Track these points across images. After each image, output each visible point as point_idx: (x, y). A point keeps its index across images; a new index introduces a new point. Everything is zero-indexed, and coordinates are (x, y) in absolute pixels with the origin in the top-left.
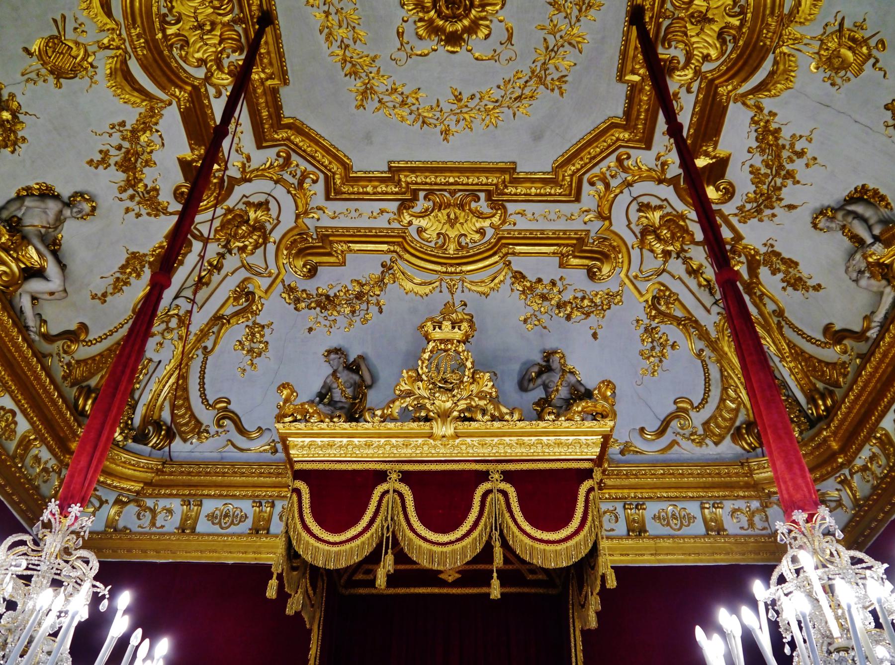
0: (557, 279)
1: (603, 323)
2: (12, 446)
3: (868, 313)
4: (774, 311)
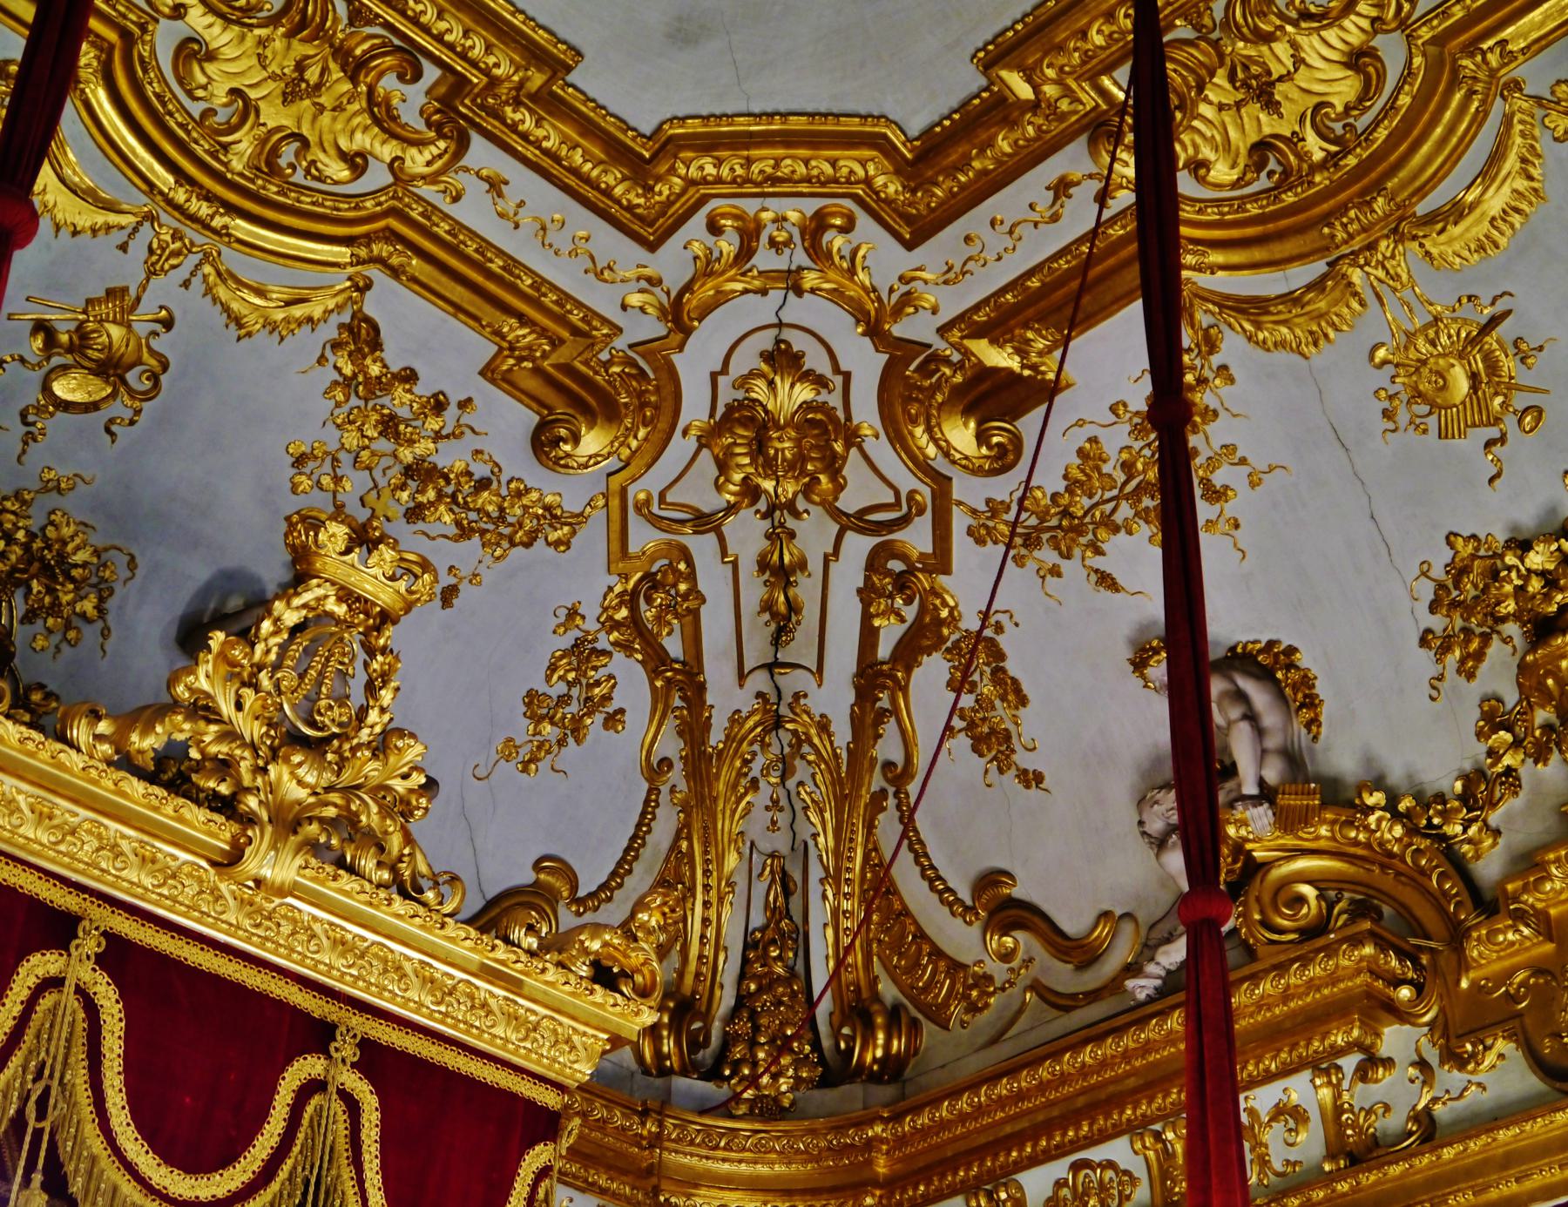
0: (455, 397)
1: (487, 576)
3: (1118, 912)
4: (889, 765)
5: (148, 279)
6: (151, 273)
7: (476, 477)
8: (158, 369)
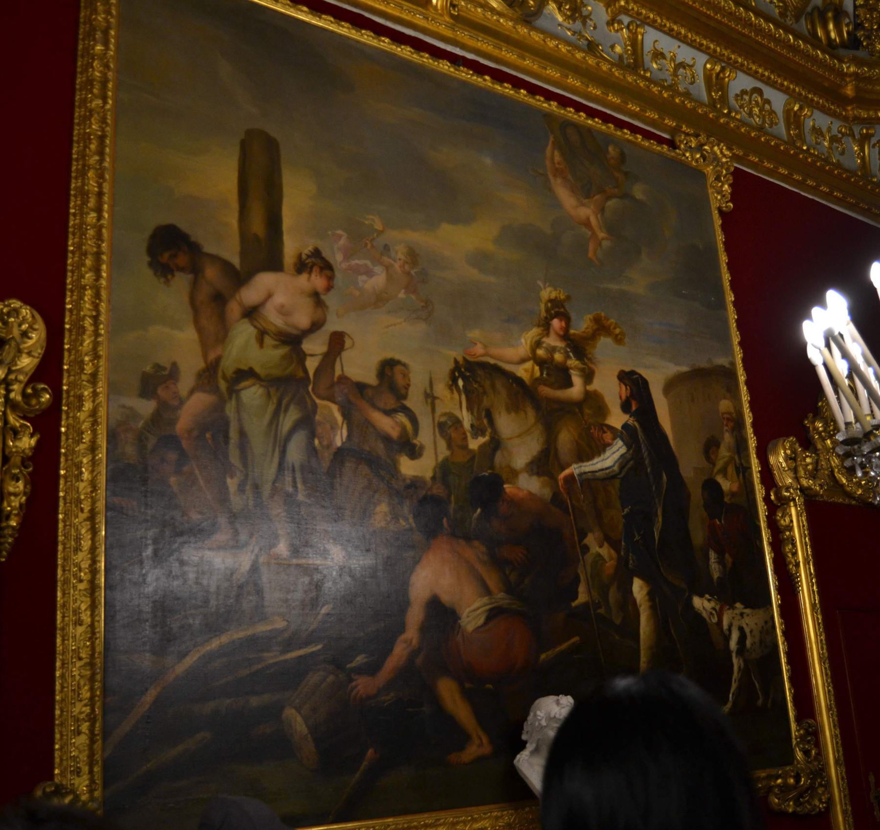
2: (781, 129)
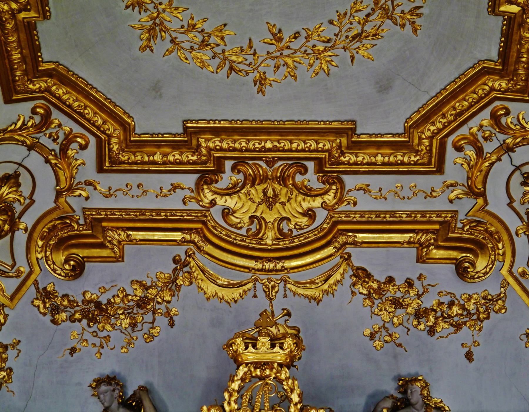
0: (414, 277)
1: (479, 338)
5: (271, 302)
6: (271, 300)
7: (446, 303)
8: (296, 333)
